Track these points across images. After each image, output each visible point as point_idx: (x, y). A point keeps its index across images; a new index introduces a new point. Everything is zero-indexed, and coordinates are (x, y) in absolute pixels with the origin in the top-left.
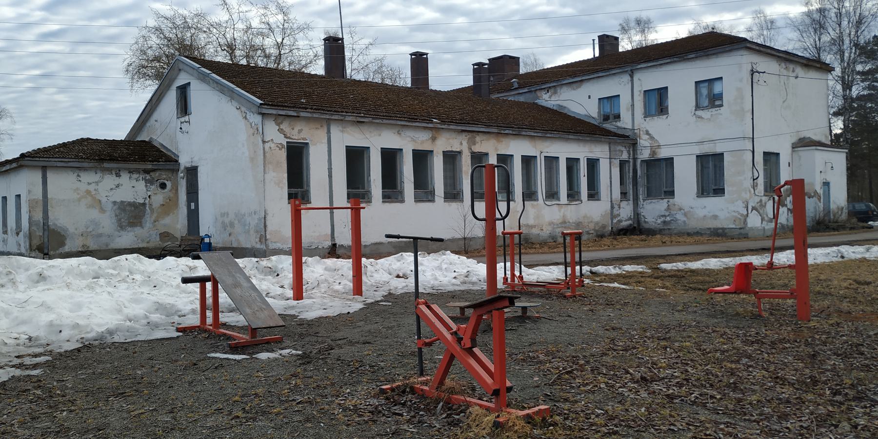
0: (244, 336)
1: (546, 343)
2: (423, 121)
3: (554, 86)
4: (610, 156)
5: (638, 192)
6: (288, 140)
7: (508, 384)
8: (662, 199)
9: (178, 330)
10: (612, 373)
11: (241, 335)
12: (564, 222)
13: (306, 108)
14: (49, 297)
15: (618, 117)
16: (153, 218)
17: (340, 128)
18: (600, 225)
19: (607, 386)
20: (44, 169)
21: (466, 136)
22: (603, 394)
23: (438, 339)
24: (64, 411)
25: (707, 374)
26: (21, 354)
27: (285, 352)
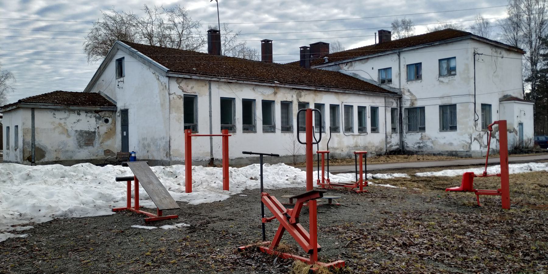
0: (154, 215)
1: (344, 221)
2: (269, 82)
3: (351, 62)
4: (385, 105)
5: (403, 128)
6: (185, 93)
7: (319, 246)
8: (418, 132)
9: (113, 210)
10: (385, 240)
11: (152, 214)
12: (356, 146)
13: (196, 74)
14: (33, 189)
15: (390, 81)
16: (100, 141)
17: (217, 86)
18: (379, 148)
19: (381, 249)
20: (33, 110)
21: (296, 92)
22: (378, 254)
23: (275, 218)
24: (40, 260)
25: (445, 242)
26: (14, 224)
27: (180, 225)
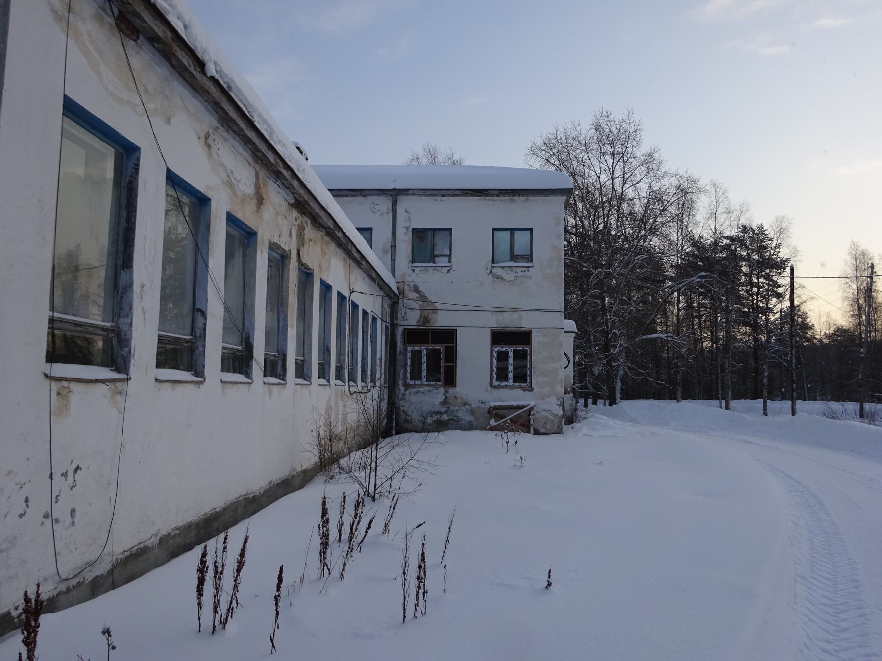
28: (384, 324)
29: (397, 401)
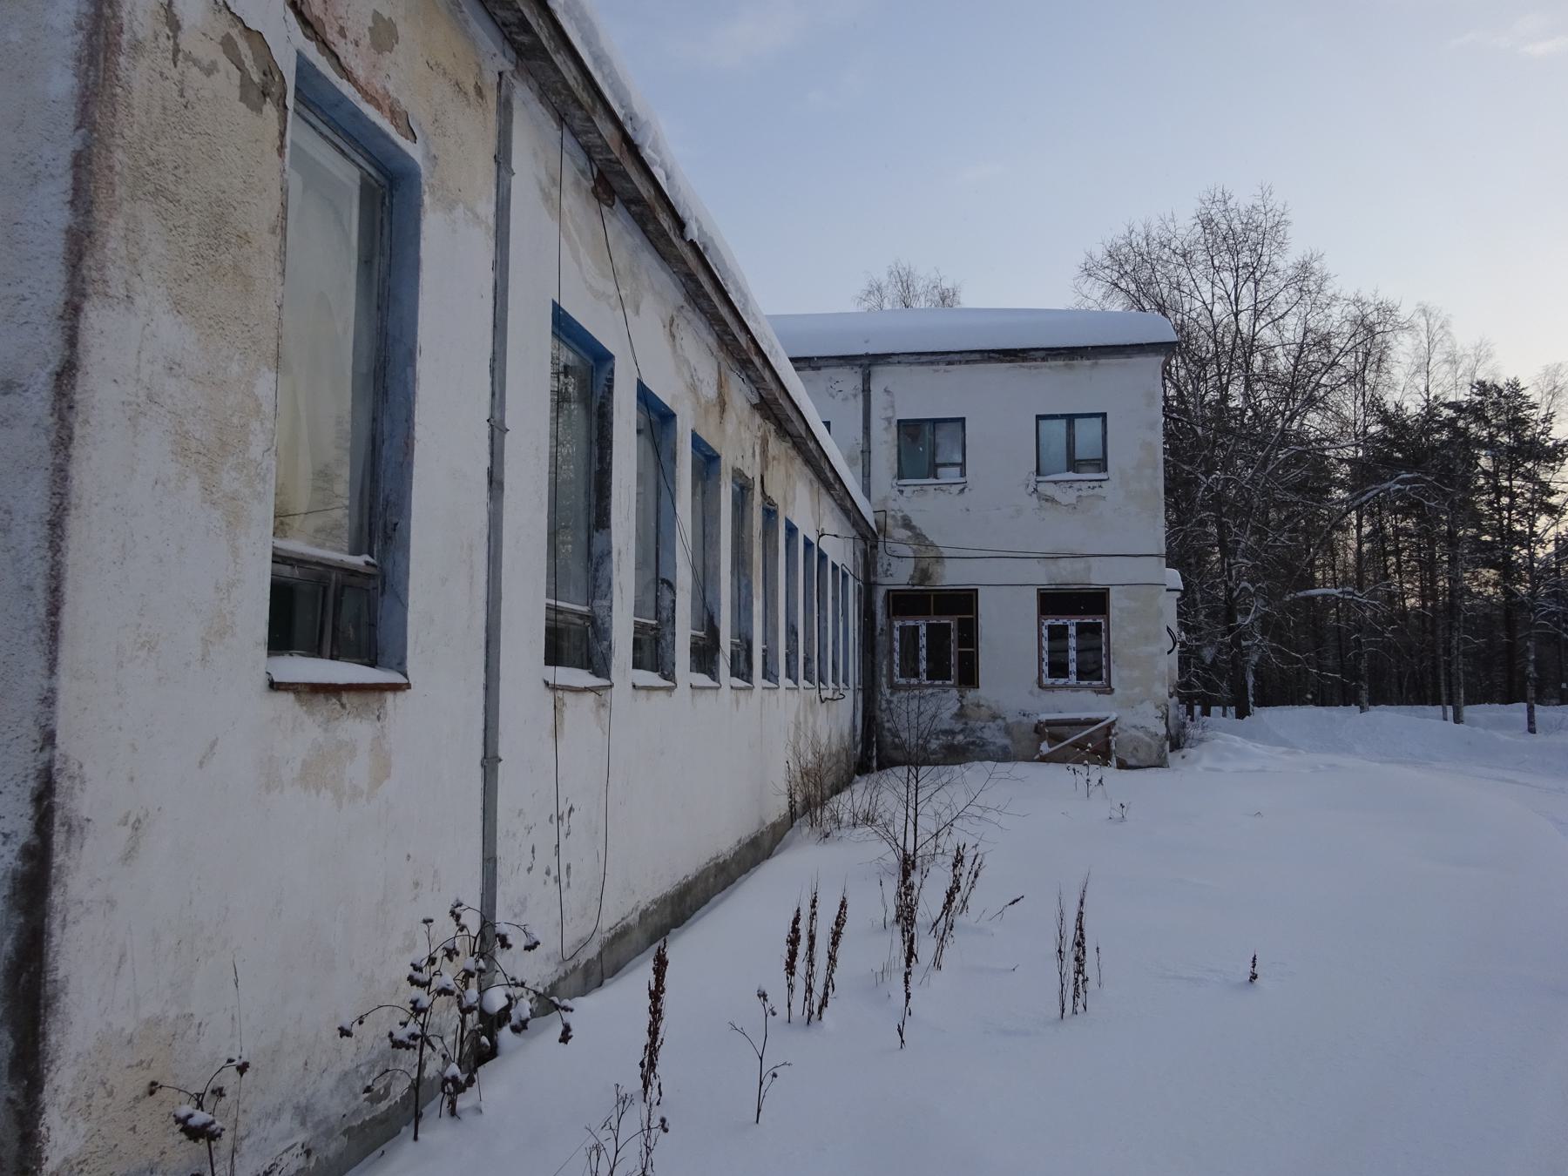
5: (877, 669)
28: (857, 583)
29: (878, 713)
